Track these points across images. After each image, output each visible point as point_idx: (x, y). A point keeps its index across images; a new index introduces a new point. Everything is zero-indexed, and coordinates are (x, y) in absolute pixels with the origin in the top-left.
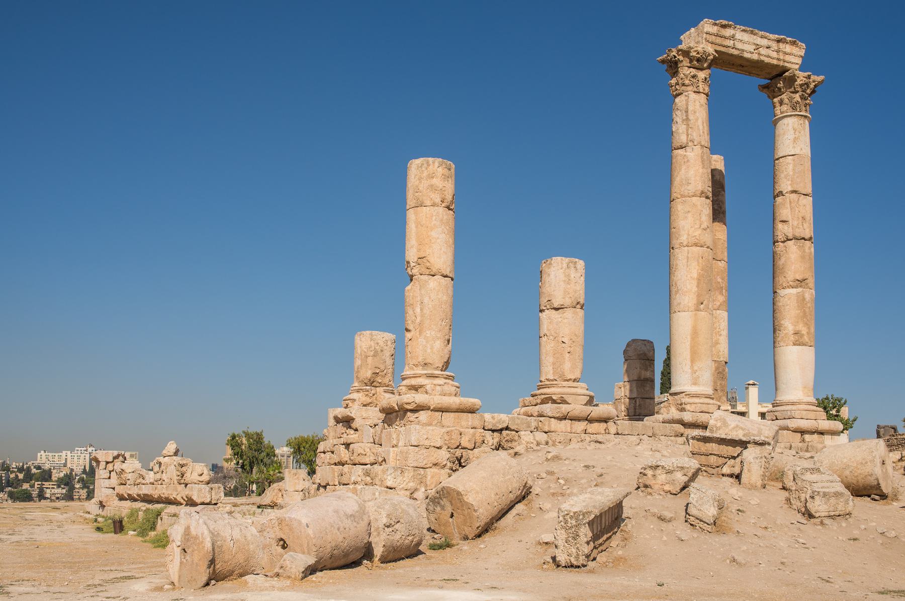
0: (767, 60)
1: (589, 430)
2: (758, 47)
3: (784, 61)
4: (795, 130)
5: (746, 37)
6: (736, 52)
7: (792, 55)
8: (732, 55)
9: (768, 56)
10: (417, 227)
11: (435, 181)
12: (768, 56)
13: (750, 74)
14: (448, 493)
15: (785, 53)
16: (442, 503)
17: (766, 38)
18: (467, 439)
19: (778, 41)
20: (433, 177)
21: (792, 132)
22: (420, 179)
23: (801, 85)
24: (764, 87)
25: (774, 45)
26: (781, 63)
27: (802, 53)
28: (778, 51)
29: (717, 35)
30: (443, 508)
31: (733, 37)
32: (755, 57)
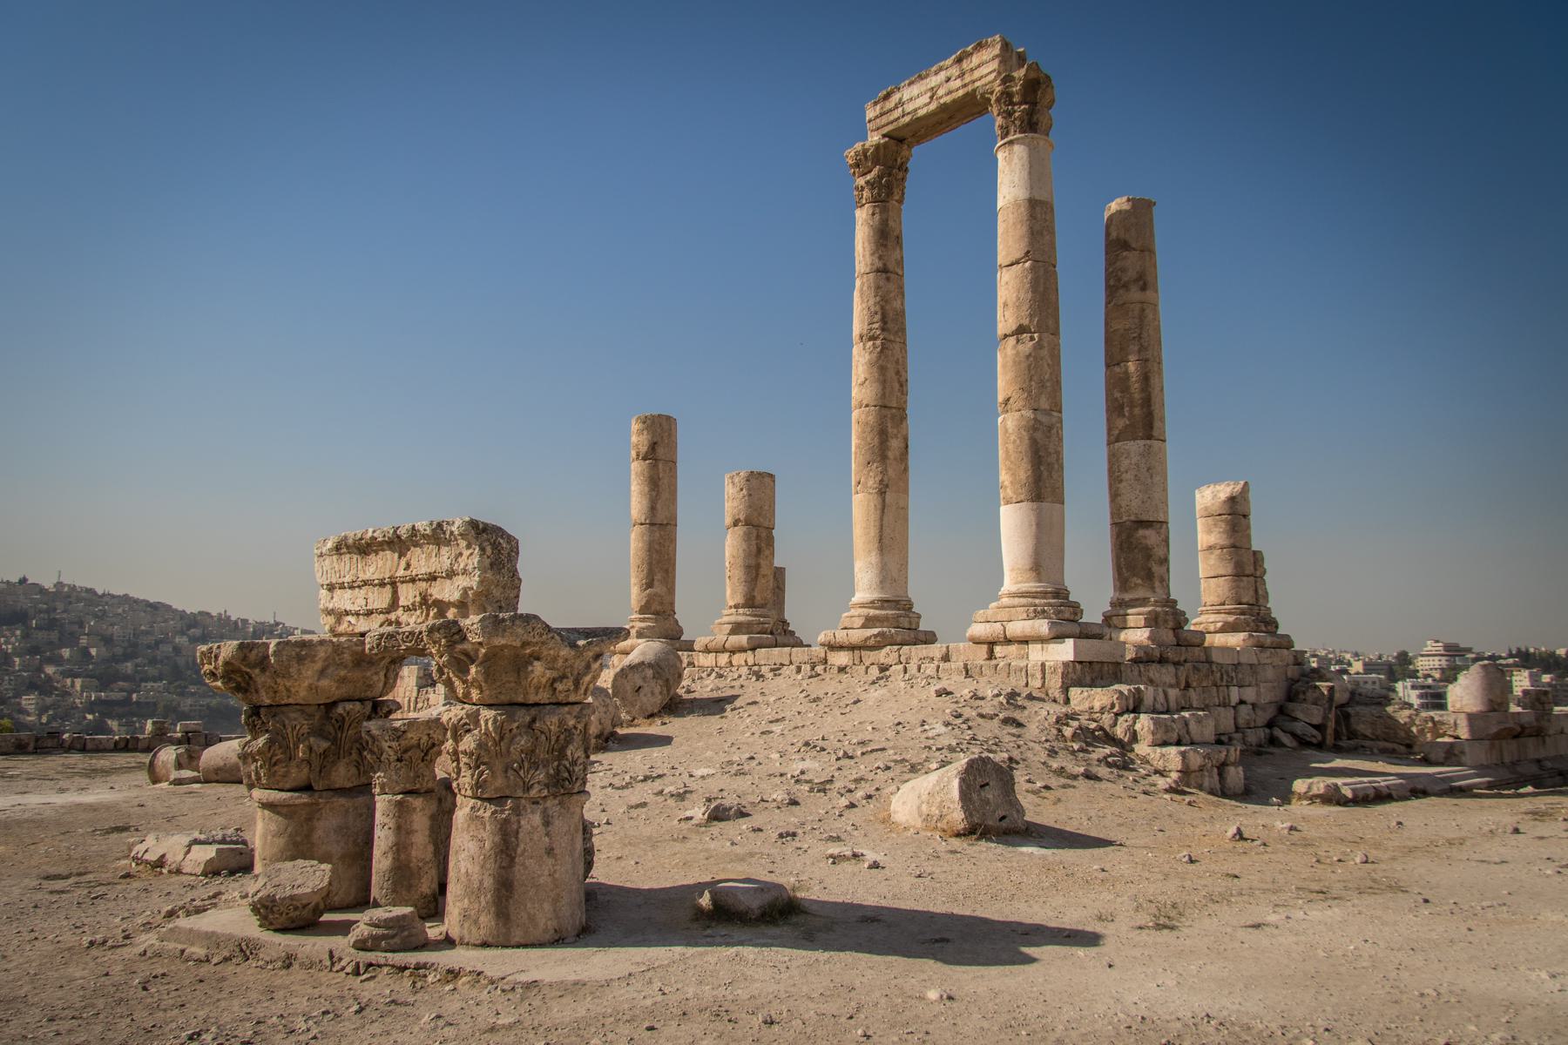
0: (948, 99)
2: (933, 91)
5: (915, 90)
6: (907, 119)
7: (984, 68)
8: (908, 125)
9: (950, 92)
12: (950, 92)
17: (941, 69)
19: (959, 60)
23: (998, 100)
25: (955, 71)
26: (970, 88)
27: (997, 51)
29: (882, 115)
31: (901, 103)
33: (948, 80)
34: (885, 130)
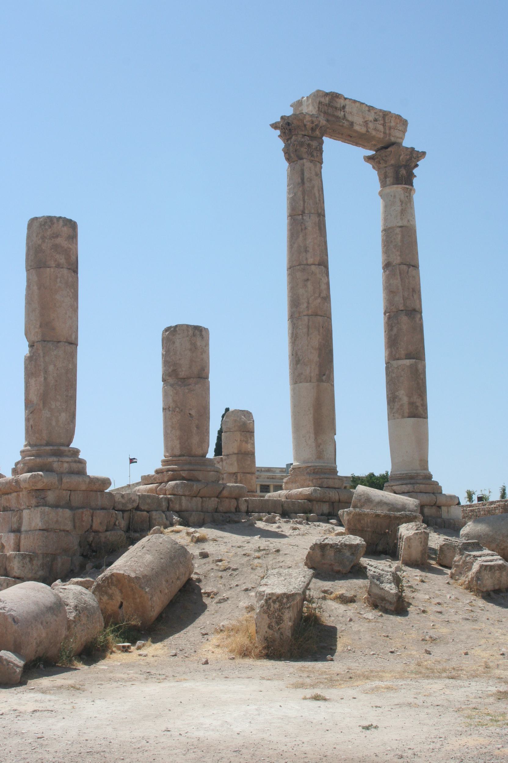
0: (374, 133)
1: (221, 509)
3: (390, 134)
4: (401, 202)
6: (346, 124)
9: (375, 129)
10: (39, 289)
11: (59, 241)
12: (375, 129)
13: (357, 144)
14: (119, 580)
15: (390, 128)
16: (110, 591)
18: (99, 521)
20: (57, 236)
21: (399, 204)
22: (43, 238)
24: (369, 159)
28: (384, 125)
30: (111, 597)
32: (363, 130)
33: (376, 120)
34: (330, 118)
